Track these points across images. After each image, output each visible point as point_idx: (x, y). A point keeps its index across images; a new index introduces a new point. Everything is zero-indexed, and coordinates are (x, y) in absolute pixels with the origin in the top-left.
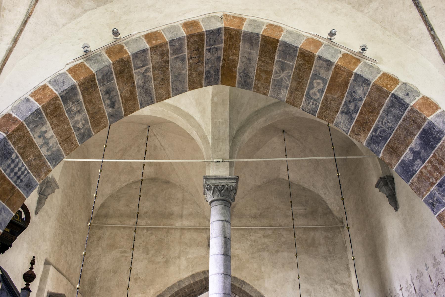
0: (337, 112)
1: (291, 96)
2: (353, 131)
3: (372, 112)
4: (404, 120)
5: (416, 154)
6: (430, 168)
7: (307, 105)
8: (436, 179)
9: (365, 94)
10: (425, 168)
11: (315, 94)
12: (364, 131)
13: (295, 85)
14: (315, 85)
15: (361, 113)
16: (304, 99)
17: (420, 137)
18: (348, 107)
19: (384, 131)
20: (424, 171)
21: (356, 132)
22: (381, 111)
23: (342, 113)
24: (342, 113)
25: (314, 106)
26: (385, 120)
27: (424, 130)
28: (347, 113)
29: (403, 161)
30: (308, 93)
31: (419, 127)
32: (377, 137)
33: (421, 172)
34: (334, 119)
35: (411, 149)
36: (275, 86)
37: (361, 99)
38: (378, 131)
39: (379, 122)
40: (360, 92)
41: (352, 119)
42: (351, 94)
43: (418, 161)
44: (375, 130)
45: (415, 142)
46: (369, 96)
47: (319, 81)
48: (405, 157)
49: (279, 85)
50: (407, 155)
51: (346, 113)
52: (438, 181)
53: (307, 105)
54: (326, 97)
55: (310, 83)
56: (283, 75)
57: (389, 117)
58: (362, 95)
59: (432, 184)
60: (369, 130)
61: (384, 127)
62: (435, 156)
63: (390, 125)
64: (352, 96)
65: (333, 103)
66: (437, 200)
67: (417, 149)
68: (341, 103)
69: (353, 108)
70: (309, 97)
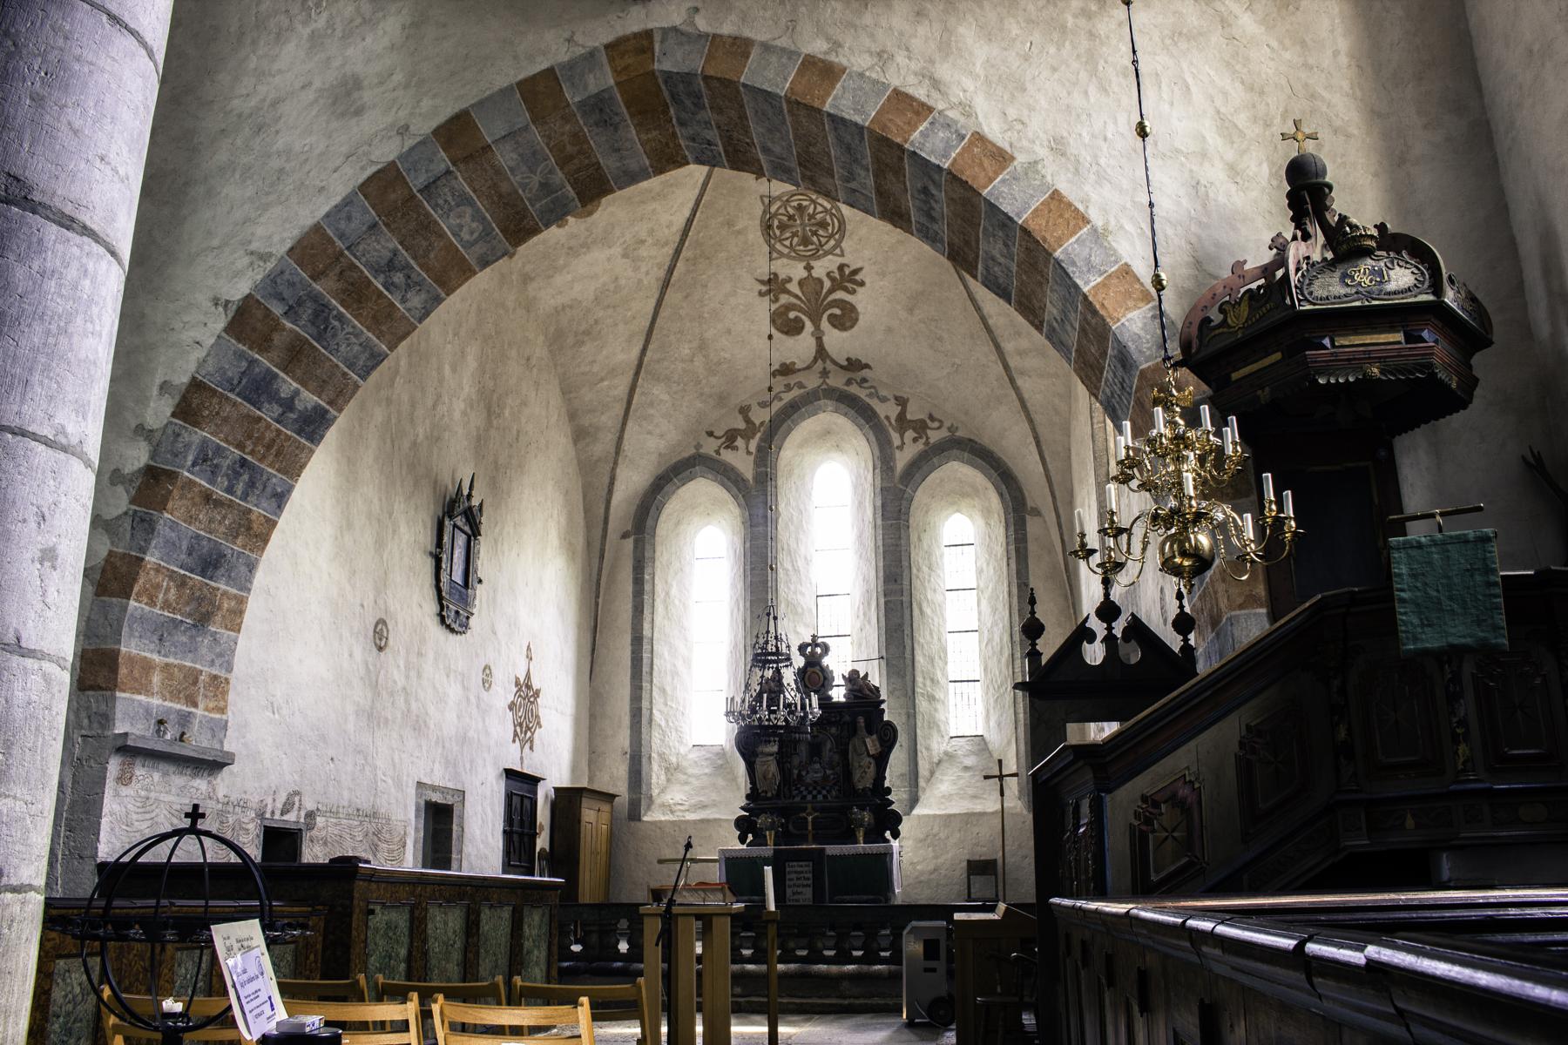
0: (401, 243)
1: (493, 167)
2: (353, 267)
3: (374, 317)
4: (345, 374)
6: (269, 435)
7: (452, 189)
8: (252, 453)
9: (409, 310)
10: (268, 426)
11: (460, 217)
12: (344, 291)
13: (504, 187)
14: (474, 225)
16: (468, 189)
17: (317, 408)
18: (401, 270)
19: (334, 336)
20: (263, 424)
21: (348, 273)
23: (395, 253)
24: (395, 253)
25: (441, 202)
26: (353, 340)
27: (327, 411)
28: (391, 266)
29: (276, 376)
30: (471, 203)
31: (330, 403)
32: (326, 320)
33: (260, 419)
34: (391, 231)
35: (297, 393)
36: (534, 153)
37: (404, 300)
38: (336, 323)
39: (354, 327)
40: (416, 300)
41: (377, 271)
42: (420, 284)
43: (277, 410)
44: (340, 317)
45: (309, 399)
46: (403, 316)
47: (476, 235)
48: (284, 381)
49: (531, 159)
50: (288, 384)
51: (391, 261)
52: (249, 458)
53: (452, 189)
54: (442, 235)
55: (484, 218)
56: (536, 180)
57: (356, 348)
58: (409, 305)
61: (341, 335)
63: (343, 348)
64: (416, 283)
65: (425, 244)
66: (216, 466)
67: (299, 406)
68: (415, 258)
69: (396, 280)
70: (464, 200)
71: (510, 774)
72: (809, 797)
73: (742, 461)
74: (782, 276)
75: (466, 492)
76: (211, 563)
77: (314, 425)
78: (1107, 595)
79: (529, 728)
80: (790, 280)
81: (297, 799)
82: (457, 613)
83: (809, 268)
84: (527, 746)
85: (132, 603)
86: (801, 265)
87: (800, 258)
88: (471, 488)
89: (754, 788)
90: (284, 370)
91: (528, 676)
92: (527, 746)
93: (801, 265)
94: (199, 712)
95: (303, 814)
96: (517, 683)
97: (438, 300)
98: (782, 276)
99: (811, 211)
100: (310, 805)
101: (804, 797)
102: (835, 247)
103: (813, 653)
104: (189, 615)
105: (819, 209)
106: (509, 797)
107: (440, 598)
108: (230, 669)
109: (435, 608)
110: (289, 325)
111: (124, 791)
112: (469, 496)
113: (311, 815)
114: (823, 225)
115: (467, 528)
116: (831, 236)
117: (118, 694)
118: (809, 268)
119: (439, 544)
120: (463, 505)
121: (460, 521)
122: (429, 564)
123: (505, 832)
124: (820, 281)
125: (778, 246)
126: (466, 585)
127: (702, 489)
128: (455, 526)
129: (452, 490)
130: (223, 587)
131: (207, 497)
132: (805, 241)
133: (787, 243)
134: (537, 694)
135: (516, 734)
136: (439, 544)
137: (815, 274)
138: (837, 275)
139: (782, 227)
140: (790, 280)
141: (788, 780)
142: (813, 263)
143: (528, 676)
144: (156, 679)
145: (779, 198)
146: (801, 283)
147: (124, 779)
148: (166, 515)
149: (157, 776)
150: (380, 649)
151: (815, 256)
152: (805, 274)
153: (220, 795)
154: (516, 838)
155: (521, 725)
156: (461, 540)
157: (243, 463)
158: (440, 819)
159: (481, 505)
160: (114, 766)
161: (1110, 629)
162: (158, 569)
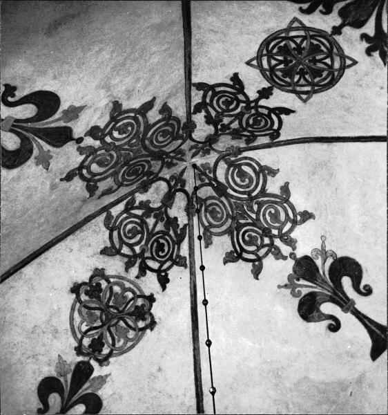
74: (365, 45)
80: (364, 37)
83: (337, 30)
86: (339, 39)
87: (334, 44)
93: (339, 39)
98: (365, 45)
99: (282, 66)
102: (297, 29)
105: (274, 62)
114: (285, 51)
116: (292, 39)
118: (337, 30)
124: (342, 13)
125: (337, 65)
132: (315, 49)
133: (328, 61)
137: (338, 22)
138: (321, 8)
139: (317, 73)
140: (364, 37)
142: (329, 30)
145: (294, 92)
146: (358, 24)
151: (321, 33)
152: (347, 30)
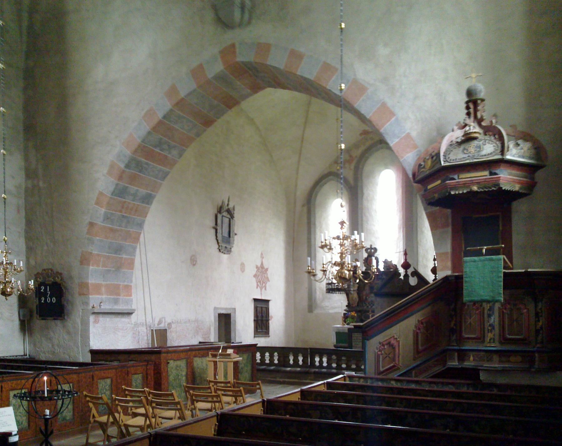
4: (154, 181)
5: (135, 195)
8: (125, 213)
10: (129, 203)
15: (160, 154)
22: (161, 167)
29: (127, 187)
31: (152, 191)
33: (125, 202)
35: (137, 190)
40: (175, 152)
44: (147, 164)
45: (143, 191)
50: (133, 189)
59: (121, 211)
60: (146, 159)
62: (139, 205)
71: (255, 300)
72: (370, 307)
73: (348, 172)
75: (226, 203)
76: (118, 250)
77: (148, 199)
78: (406, 259)
79: (263, 282)
81: (163, 320)
82: (226, 247)
84: (264, 289)
85: (91, 267)
88: (228, 201)
89: (349, 303)
90: (130, 184)
91: (262, 264)
92: (264, 289)
94: (121, 297)
95: (166, 324)
96: (257, 267)
97: (184, 151)
100: (169, 320)
101: (368, 307)
103: (371, 251)
104: (113, 267)
106: (256, 308)
107: (218, 243)
108: (131, 282)
109: (217, 246)
110: (128, 170)
111: (97, 325)
112: (228, 205)
113: (170, 324)
115: (229, 216)
117: (90, 296)
119: (216, 224)
120: (226, 208)
121: (225, 214)
122: (213, 231)
123: (254, 320)
126: (230, 236)
127: (328, 187)
128: (223, 216)
129: (220, 204)
130: (124, 256)
131: (112, 230)
134: (267, 270)
135: (258, 285)
136: (216, 224)
141: (361, 300)
143: (262, 264)
144: (103, 289)
147: (96, 322)
148: (98, 238)
149: (108, 319)
150: (194, 265)
153: (133, 322)
154: (260, 322)
155: (260, 282)
156: (226, 220)
157: (123, 216)
158: (225, 321)
159: (234, 207)
160: (92, 318)
161: (406, 272)
162: (98, 255)
